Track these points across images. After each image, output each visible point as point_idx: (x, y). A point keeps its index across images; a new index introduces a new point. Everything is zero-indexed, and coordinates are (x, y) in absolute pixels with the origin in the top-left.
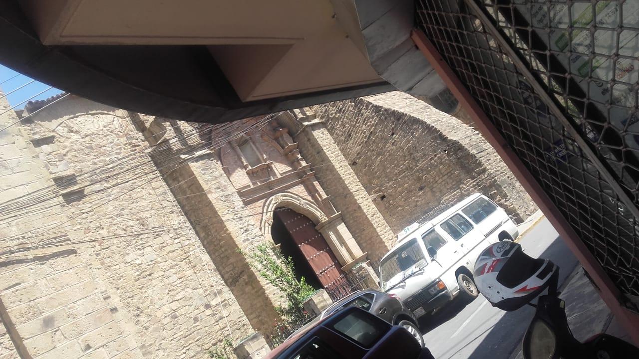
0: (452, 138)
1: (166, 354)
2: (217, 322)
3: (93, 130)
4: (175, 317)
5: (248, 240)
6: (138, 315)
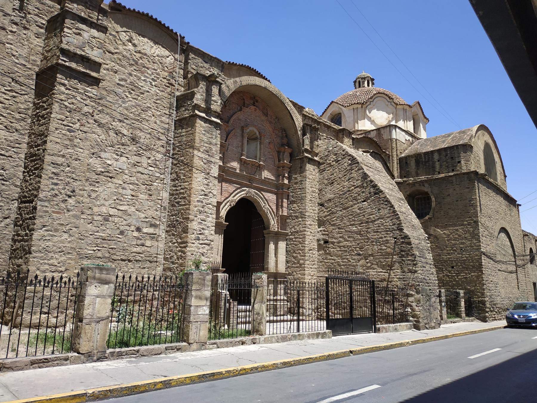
0: (407, 232)
1: (69, 240)
2: (137, 245)
3: (148, 52)
4: (106, 220)
5: (202, 202)
6: (70, 197)
